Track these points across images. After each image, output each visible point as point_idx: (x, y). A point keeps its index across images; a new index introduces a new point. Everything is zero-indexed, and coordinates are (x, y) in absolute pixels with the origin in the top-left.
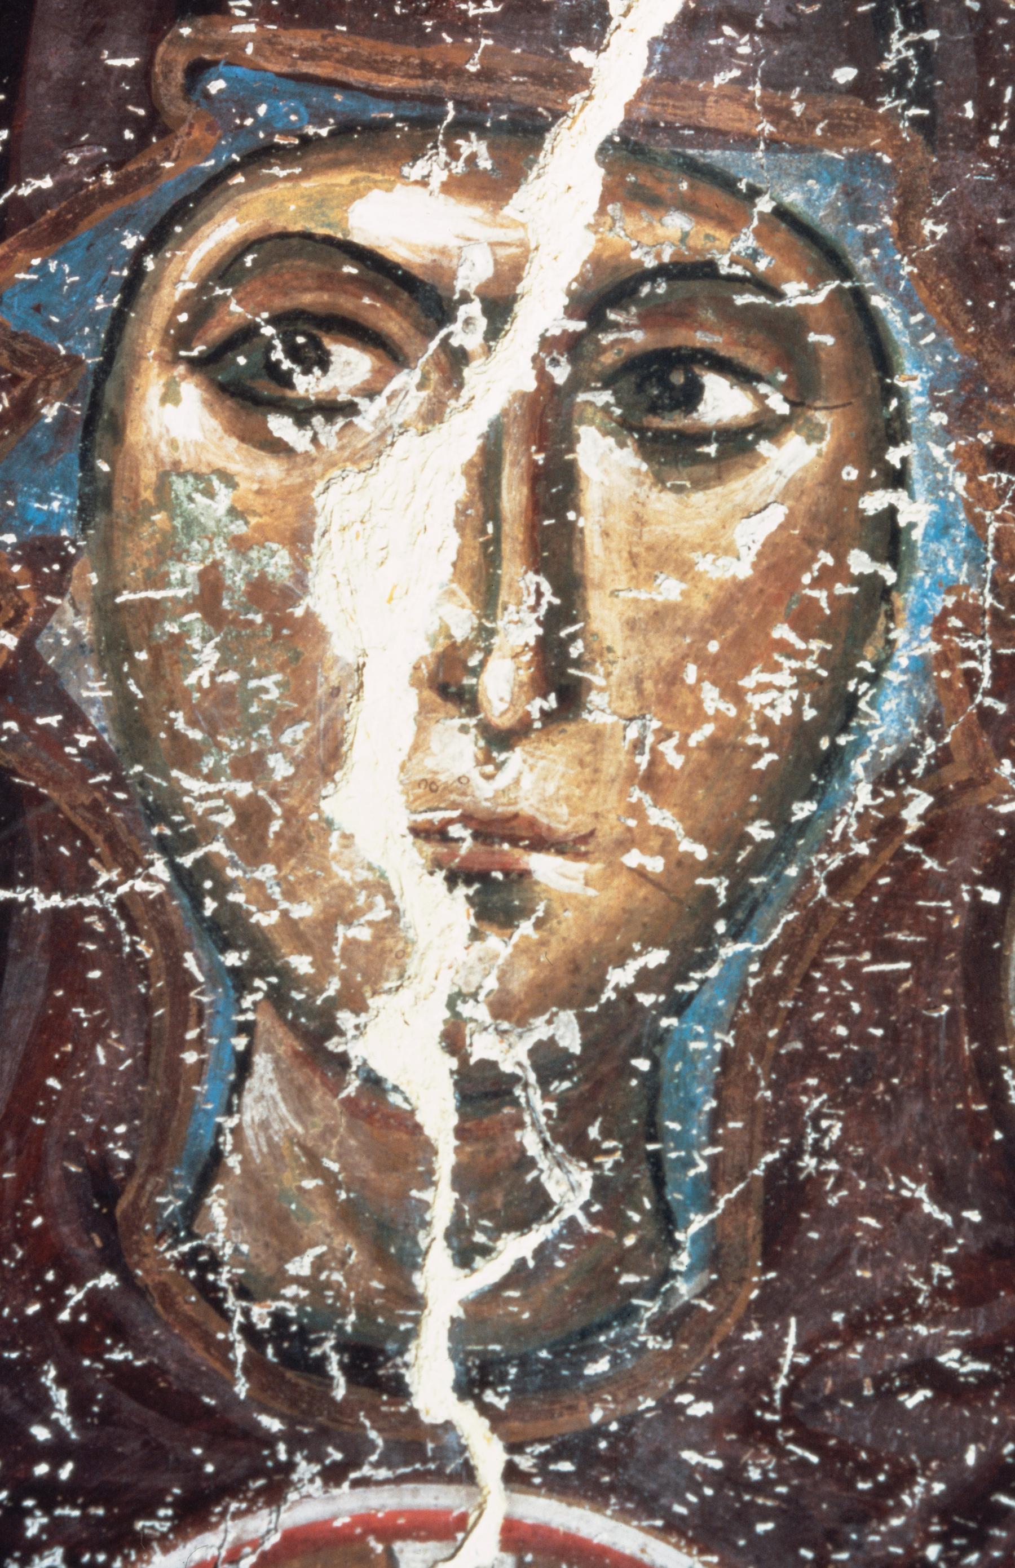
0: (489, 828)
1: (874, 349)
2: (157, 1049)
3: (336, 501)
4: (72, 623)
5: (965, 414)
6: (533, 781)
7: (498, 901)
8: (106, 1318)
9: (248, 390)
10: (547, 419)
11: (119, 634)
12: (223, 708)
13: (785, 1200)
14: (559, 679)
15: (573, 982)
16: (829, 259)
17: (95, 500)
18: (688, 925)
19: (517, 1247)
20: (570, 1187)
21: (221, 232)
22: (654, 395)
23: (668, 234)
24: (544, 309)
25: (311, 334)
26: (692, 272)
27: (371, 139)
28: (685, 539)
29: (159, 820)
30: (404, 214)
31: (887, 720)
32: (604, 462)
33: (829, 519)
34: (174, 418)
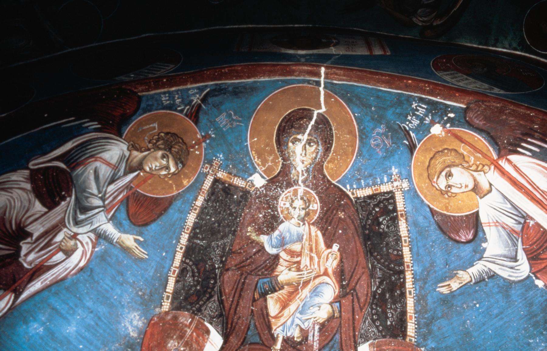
0: (303, 161)
1: (318, 142)
2: (289, 169)
3: (296, 148)
4: (286, 152)
5: (322, 144)
6: (304, 159)
7: (303, 163)
8: (287, 180)
9: (293, 143)
10: (305, 145)
11: (288, 153)
12: (292, 156)
13: (314, 176)
14: (305, 155)
15: (306, 167)
16: (316, 138)
17: (287, 148)
18: (311, 164)
19: (304, 177)
20: (306, 175)
21: (292, 137)
22: (309, 144)
23: (310, 138)
24: (305, 140)
25: (296, 141)
26: (311, 139)
27: (298, 134)
28: (311, 149)
29: (289, 160)
30: (299, 137)
31: (319, 157)
32: (307, 146)
33: (316, 149)
34: (290, 144)
